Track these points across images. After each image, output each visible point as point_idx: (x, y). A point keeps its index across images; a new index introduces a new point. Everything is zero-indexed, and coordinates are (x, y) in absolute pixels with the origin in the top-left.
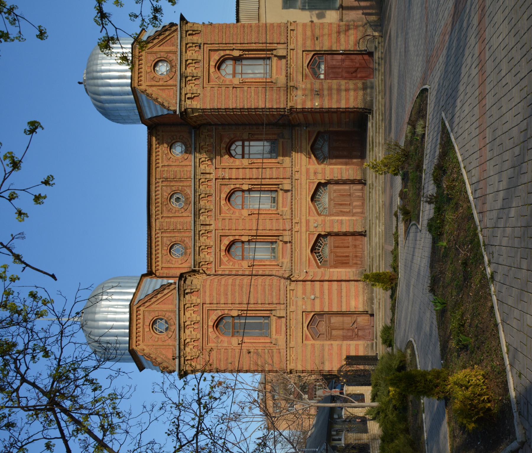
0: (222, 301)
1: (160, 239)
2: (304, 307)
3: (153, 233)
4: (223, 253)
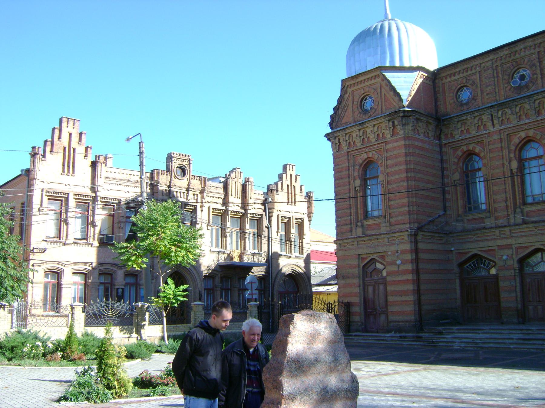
0: (390, 162)
1: (473, 71)
2: (389, 253)
3: (478, 62)
4: (465, 149)
